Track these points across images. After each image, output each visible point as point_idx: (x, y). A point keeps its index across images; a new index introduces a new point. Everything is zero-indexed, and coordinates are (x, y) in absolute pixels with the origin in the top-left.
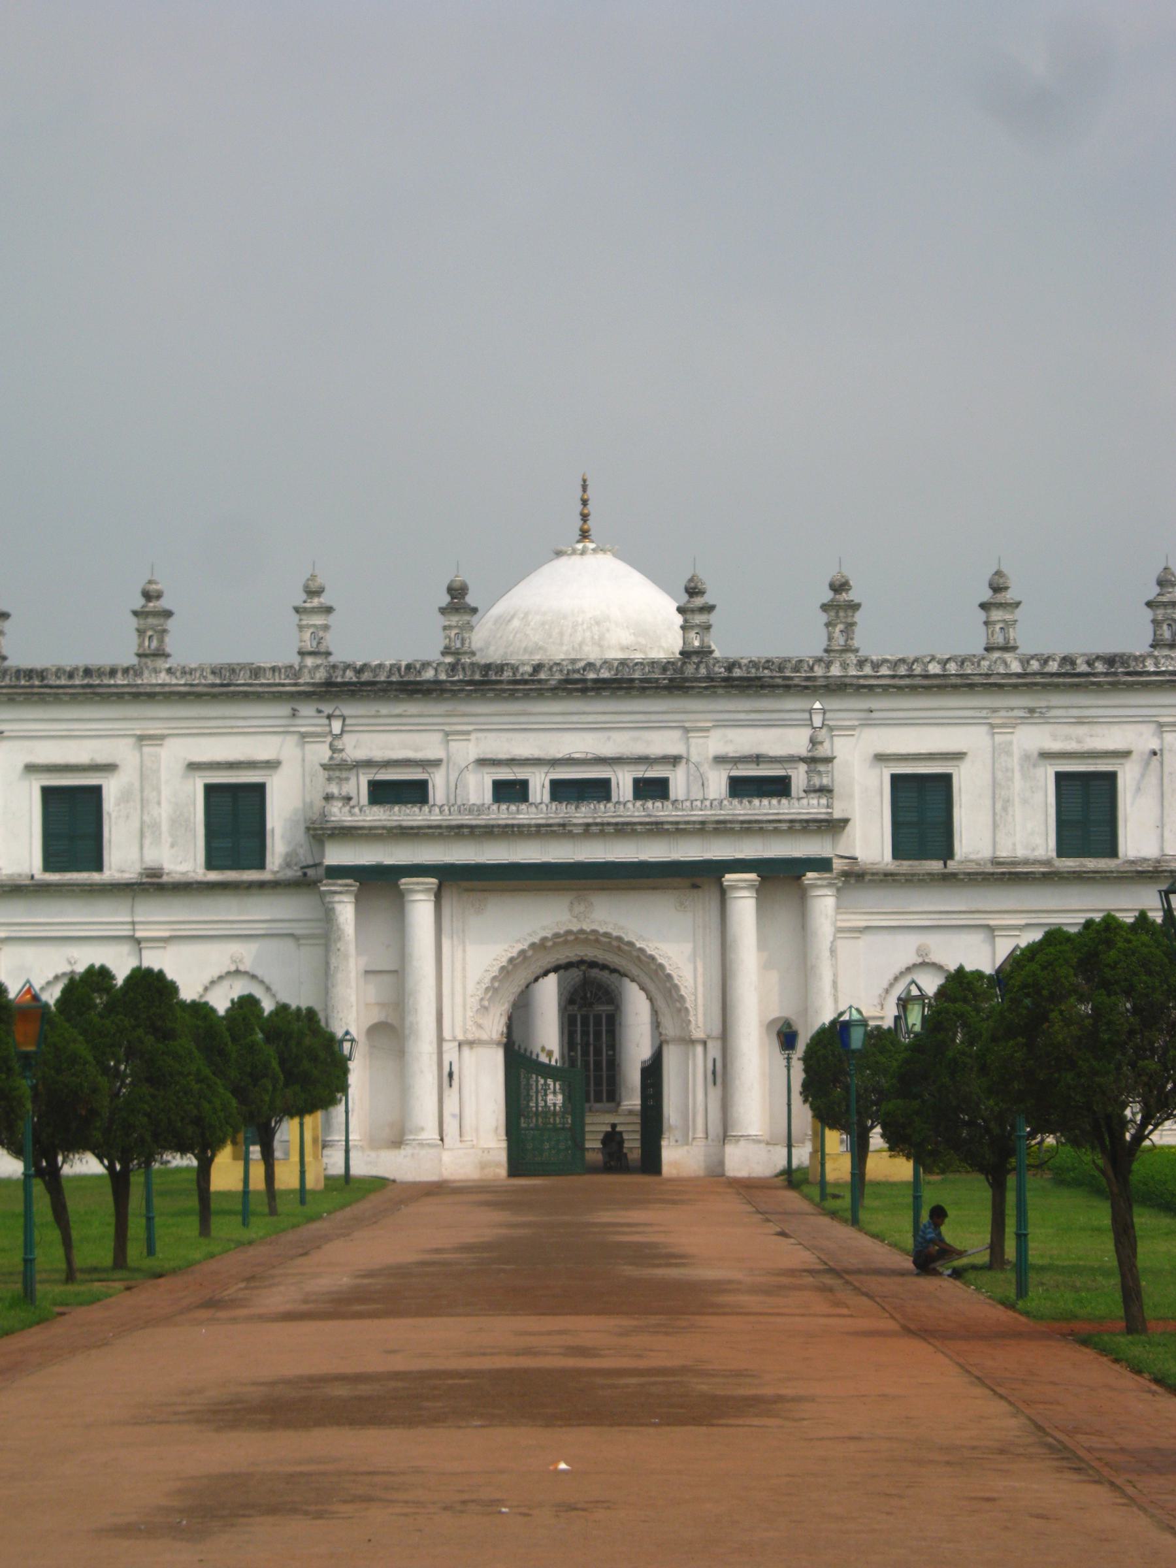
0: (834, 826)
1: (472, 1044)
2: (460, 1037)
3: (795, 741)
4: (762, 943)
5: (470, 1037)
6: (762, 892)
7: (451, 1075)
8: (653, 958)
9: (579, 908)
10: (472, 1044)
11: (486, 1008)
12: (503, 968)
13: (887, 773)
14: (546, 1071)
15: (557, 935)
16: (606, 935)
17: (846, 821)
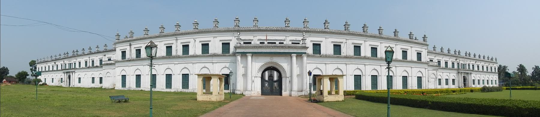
0: (306, 48)
1: (256, 77)
2: (255, 76)
3: (300, 38)
4: (297, 64)
5: (256, 76)
6: (297, 56)
7: (253, 81)
8: (281, 66)
9: (271, 59)
10: (256, 77)
11: (258, 72)
12: (261, 67)
13: (312, 43)
14: (266, 81)
15: (268, 62)
16: (275, 62)
17: (308, 47)
